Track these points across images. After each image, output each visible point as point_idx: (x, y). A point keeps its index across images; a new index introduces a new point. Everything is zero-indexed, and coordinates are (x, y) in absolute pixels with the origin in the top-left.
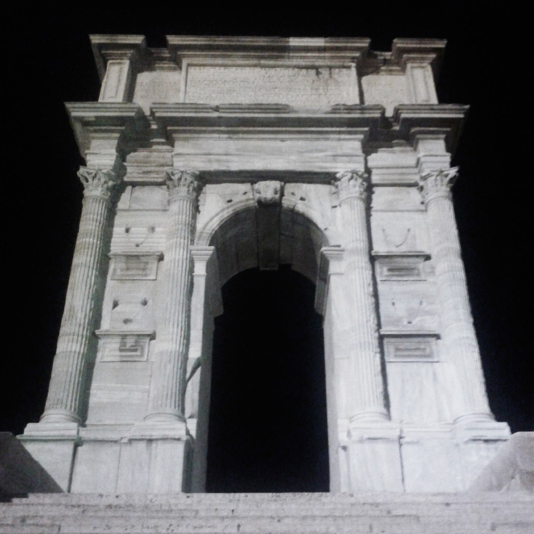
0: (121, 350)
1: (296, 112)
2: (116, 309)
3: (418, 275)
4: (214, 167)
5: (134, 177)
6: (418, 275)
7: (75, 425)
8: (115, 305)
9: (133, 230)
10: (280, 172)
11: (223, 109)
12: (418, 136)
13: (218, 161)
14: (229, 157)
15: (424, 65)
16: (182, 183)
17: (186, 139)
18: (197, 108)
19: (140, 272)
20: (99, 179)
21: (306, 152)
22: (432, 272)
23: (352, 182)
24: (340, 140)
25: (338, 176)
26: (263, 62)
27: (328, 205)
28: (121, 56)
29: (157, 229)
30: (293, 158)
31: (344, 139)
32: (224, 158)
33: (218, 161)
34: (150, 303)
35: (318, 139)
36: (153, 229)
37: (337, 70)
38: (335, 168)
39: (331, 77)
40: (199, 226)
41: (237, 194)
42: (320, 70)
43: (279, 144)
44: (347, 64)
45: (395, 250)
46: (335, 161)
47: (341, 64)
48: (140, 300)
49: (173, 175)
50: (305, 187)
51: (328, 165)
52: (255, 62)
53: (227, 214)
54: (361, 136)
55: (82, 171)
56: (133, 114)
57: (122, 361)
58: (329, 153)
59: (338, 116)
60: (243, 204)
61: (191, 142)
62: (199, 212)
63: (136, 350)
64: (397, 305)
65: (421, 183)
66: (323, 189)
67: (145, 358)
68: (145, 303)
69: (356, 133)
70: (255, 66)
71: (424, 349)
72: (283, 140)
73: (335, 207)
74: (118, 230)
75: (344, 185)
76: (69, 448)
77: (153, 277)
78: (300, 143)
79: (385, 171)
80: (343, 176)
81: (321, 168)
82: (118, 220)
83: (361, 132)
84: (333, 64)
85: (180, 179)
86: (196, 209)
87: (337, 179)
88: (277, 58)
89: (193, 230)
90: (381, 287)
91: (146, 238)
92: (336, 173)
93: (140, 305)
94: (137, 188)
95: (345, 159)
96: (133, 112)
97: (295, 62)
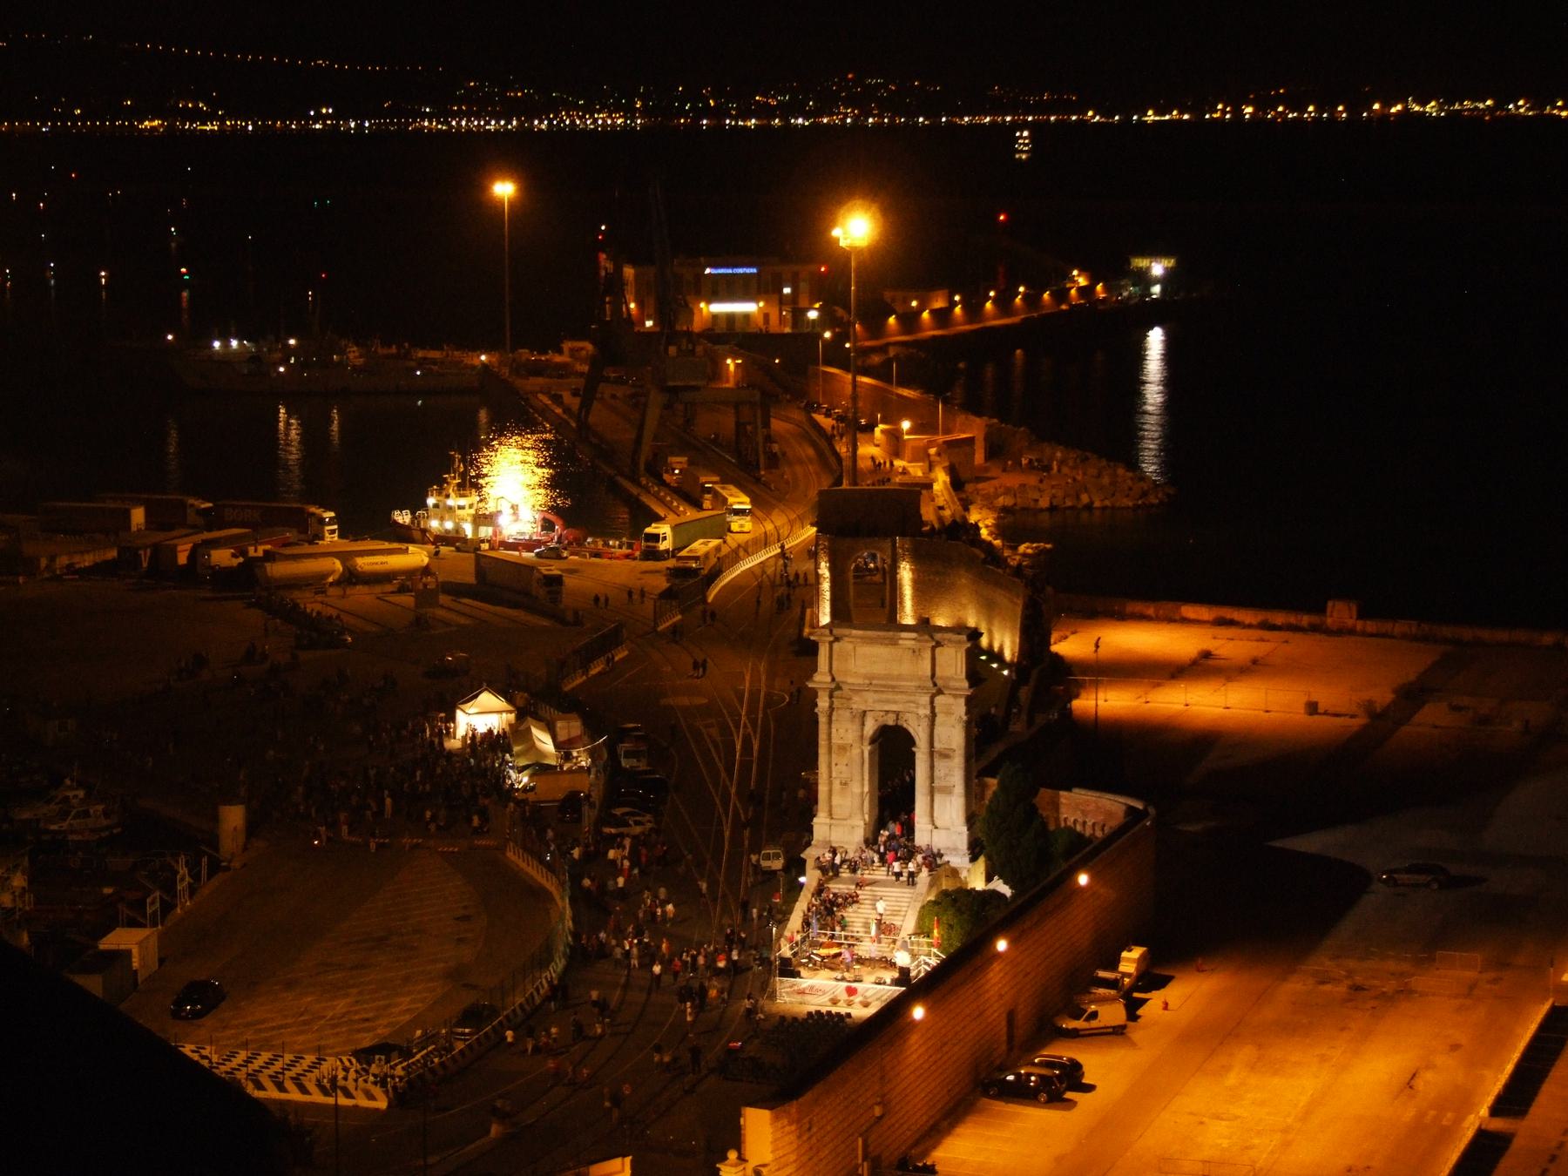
2: (838, 767)
8: (836, 765)
29: (850, 731)
36: (847, 731)
40: (865, 732)
53: (875, 728)
55: (816, 710)
74: (834, 730)
82: (833, 726)
86: (863, 724)
89: (862, 736)
90: (936, 764)
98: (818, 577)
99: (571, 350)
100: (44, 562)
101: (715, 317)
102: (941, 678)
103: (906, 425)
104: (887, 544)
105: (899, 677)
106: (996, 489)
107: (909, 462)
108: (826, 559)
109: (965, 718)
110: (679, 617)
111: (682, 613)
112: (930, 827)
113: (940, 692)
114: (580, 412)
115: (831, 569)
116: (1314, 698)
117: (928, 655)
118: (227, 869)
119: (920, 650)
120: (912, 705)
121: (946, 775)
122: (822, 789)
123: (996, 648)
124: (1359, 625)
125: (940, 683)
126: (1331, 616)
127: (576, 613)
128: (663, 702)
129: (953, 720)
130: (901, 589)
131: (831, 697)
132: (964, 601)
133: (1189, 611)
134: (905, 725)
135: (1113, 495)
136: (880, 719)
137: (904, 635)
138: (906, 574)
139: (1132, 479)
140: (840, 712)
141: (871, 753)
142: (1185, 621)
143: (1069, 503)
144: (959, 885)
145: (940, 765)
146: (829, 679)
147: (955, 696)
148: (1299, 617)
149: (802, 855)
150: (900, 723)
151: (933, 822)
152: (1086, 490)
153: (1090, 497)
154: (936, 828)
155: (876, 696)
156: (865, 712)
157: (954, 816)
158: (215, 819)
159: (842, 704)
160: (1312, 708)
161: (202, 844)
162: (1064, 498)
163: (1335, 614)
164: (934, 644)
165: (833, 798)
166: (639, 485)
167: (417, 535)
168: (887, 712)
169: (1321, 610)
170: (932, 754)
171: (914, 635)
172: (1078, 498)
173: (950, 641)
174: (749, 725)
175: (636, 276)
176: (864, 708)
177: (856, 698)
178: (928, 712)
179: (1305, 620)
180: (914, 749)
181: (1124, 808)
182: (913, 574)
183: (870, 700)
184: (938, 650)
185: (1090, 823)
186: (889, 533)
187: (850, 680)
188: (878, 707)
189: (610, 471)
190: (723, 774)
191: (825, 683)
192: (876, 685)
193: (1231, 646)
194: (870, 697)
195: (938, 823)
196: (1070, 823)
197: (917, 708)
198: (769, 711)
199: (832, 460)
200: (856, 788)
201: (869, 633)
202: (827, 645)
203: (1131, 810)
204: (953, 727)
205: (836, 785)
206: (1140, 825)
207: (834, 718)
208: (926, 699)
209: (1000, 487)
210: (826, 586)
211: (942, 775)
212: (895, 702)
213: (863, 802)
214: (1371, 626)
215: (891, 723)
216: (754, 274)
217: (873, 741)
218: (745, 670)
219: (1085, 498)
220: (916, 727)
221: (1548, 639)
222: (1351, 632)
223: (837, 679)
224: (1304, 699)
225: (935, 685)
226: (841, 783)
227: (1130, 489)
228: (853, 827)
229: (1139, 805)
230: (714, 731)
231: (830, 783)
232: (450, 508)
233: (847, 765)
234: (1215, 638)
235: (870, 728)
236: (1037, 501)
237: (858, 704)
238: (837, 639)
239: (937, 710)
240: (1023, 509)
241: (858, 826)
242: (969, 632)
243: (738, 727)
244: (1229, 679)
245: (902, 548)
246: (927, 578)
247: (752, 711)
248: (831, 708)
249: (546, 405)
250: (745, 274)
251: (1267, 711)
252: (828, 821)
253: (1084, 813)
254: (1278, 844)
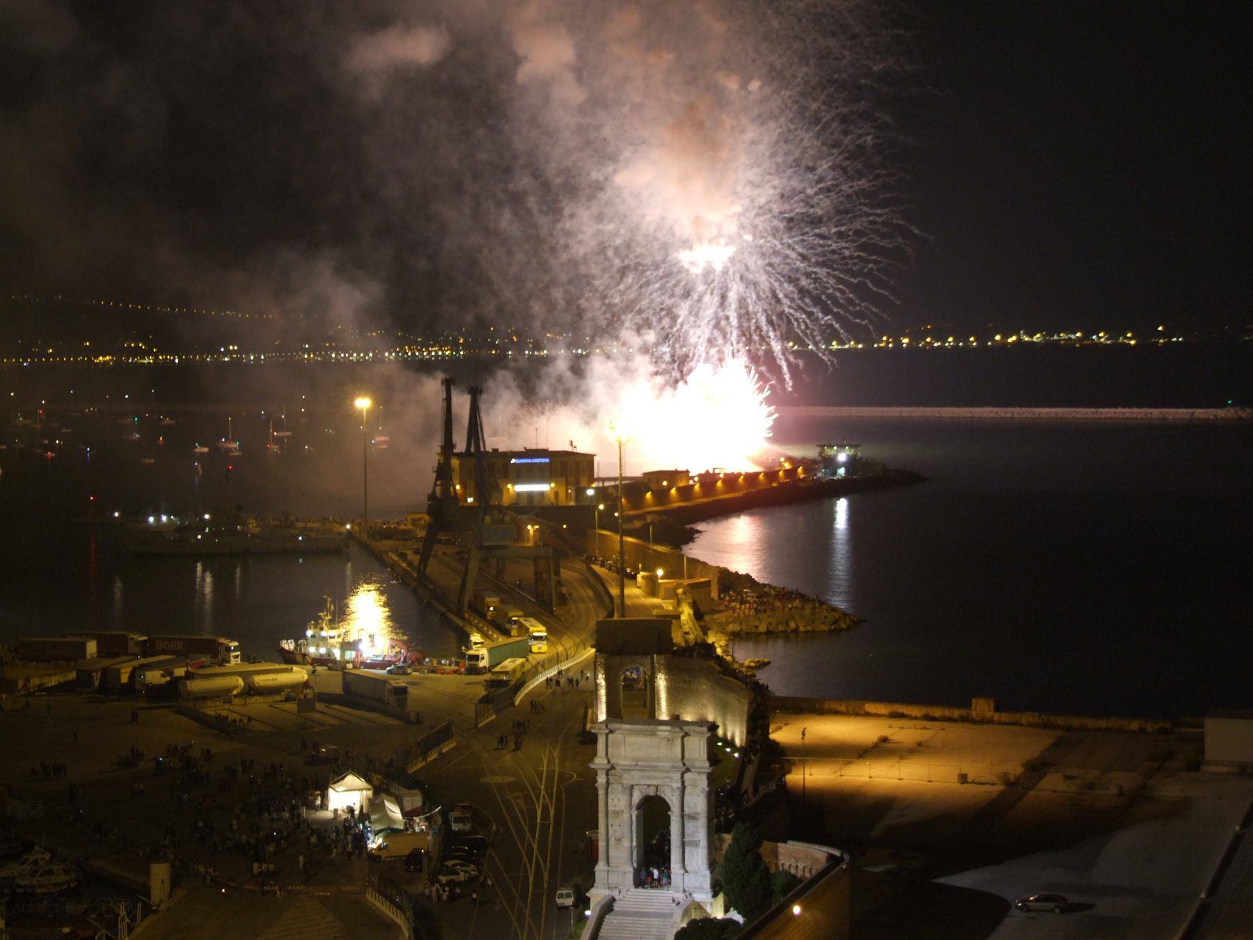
2: (614, 827)
27: (671, 794)
36: (619, 800)
40: (633, 802)
53: (641, 797)
55: (596, 785)
66: (669, 788)
74: (610, 800)
86: (631, 795)
98: (596, 685)
99: (413, 520)
100: (21, 683)
101: (519, 494)
102: (689, 759)
103: (660, 572)
104: (648, 660)
105: (658, 759)
106: (727, 618)
107: (663, 599)
108: (603, 672)
109: (707, 789)
110: (494, 716)
111: (496, 714)
112: (682, 871)
113: (688, 770)
114: (420, 564)
115: (607, 680)
116: (964, 771)
117: (679, 742)
118: (156, 912)
119: (673, 739)
120: (668, 780)
121: (694, 832)
122: (602, 844)
123: (729, 736)
124: (996, 716)
125: (688, 763)
126: (975, 710)
127: (418, 715)
128: (483, 780)
129: (698, 791)
130: (658, 694)
131: (607, 774)
132: (705, 701)
133: (871, 707)
134: (662, 796)
135: (813, 622)
136: (644, 792)
137: (661, 728)
138: (661, 682)
139: (826, 610)
140: (615, 786)
141: (638, 817)
142: (868, 715)
143: (781, 628)
144: (704, 915)
145: (689, 825)
146: (605, 761)
147: (699, 773)
148: (952, 710)
149: (587, 895)
150: (659, 793)
151: (684, 867)
152: (793, 618)
153: (796, 623)
154: (687, 872)
155: (640, 774)
156: (632, 786)
157: (700, 863)
158: (147, 873)
160: (963, 778)
161: (137, 893)
162: (777, 625)
163: (978, 708)
164: (683, 734)
165: (610, 851)
166: (463, 618)
167: (299, 658)
168: (649, 785)
169: (967, 705)
170: (683, 816)
171: (668, 728)
172: (787, 624)
173: (695, 732)
174: (546, 796)
175: (461, 465)
176: (631, 783)
177: (626, 776)
178: (679, 785)
179: (956, 713)
180: (669, 813)
181: (826, 855)
182: (667, 682)
183: (636, 777)
184: (686, 739)
185: (801, 867)
186: (647, 653)
187: (621, 762)
188: (642, 782)
189: (443, 609)
190: (528, 835)
191: (603, 764)
192: (641, 766)
193: (901, 733)
194: (636, 774)
195: (688, 868)
196: (786, 867)
197: (672, 782)
198: (561, 786)
199: (606, 599)
200: (626, 843)
201: (635, 727)
202: (604, 737)
203: (831, 856)
204: (698, 796)
205: (612, 841)
206: (837, 869)
207: (609, 791)
208: (678, 775)
209: (730, 617)
210: (603, 692)
212: (655, 778)
213: (632, 853)
214: (1004, 717)
215: (652, 794)
216: (547, 463)
217: (639, 807)
218: (543, 756)
219: (792, 625)
220: (671, 797)
221: (1134, 725)
222: (991, 722)
223: (612, 762)
224: (957, 772)
225: (684, 764)
226: (616, 840)
227: (826, 617)
228: (625, 873)
229: (837, 853)
230: (520, 802)
231: (608, 840)
232: (324, 639)
233: (620, 826)
234: (890, 727)
235: (637, 797)
236: (757, 627)
237: (627, 779)
238: (611, 732)
239: (686, 784)
240: (747, 633)
242: (709, 724)
243: (538, 798)
244: (901, 758)
245: (659, 664)
246: (677, 685)
247: (549, 786)
248: (608, 783)
249: (394, 561)
250: (540, 463)
251: (930, 781)
252: (606, 868)
253: (797, 860)
254: (942, 881)
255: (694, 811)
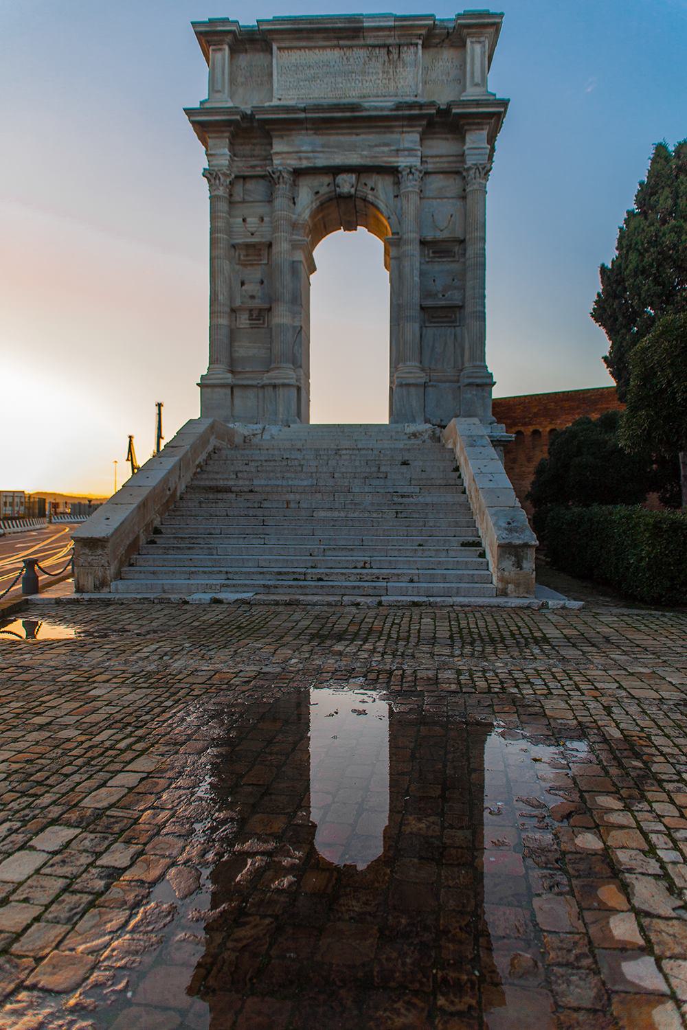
0: (250, 320)
1: (366, 110)
2: (243, 287)
3: (454, 257)
4: (305, 164)
5: (244, 172)
6: (454, 257)
7: (229, 375)
8: (243, 284)
9: (249, 220)
10: (357, 166)
11: (309, 109)
12: (466, 127)
13: (307, 158)
14: (316, 154)
15: (482, 39)
16: (281, 180)
17: (282, 137)
18: (287, 109)
19: (256, 258)
20: (219, 179)
21: (376, 146)
22: (464, 254)
23: (411, 177)
24: (403, 132)
25: (400, 169)
26: (341, 42)
28: (221, 43)
29: (265, 219)
30: (365, 153)
31: (406, 132)
32: (311, 155)
33: (307, 158)
34: (265, 282)
35: (385, 133)
36: (262, 220)
37: (405, 48)
38: (398, 162)
39: (399, 57)
41: (322, 186)
42: (391, 48)
43: (354, 138)
44: (414, 41)
45: (441, 235)
46: (398, 156)
47: (409, 41)
48: (259, 280)
49: (274, 173)
50: (375, 177)
51: (393, 159)
52: (335, 42)
54: (420, 129)
56: (238, 117)
57: (252, 328)
58: (393, 148)
59: (400, 113)
60: (327, 196)
61: (285, 138)
62: (294, 203)
63: (259, 320)
64: (436, 282)
65: (464, 174)
66: (389, 180)
67: (266, 325)
68: (262, 282)
69: (415, 126)
70: (334, 47)
71: (451, 317)
72: (357, 135)
73: (396, 196)
75: (405, 178)
76: (228, 391)
77: (265, 262)
78: (371, 137)
79: (438, 159)
80: (404, 170)
81: (386, 162)
83: (420, 126)
84: (402, 42)
85: (279, 178)
87: (398, 172)
88: (353, 38)
91: (258, 227)
92: (398, 167)
93: (259, 284)
94: (247, 180)
95: (406, 153)
96: (238, 115)
97: (370, 41)
120: (386, 149)
156: (298, 173)
159: (253, 167)
168: (335, 171)
176: (293, 163)
178: (416, 162)
207: (237, 198)
211: (440, 288)
212: (353, 148)
233: (262, 282)
241: (284, 385)
255: (445, 235)
